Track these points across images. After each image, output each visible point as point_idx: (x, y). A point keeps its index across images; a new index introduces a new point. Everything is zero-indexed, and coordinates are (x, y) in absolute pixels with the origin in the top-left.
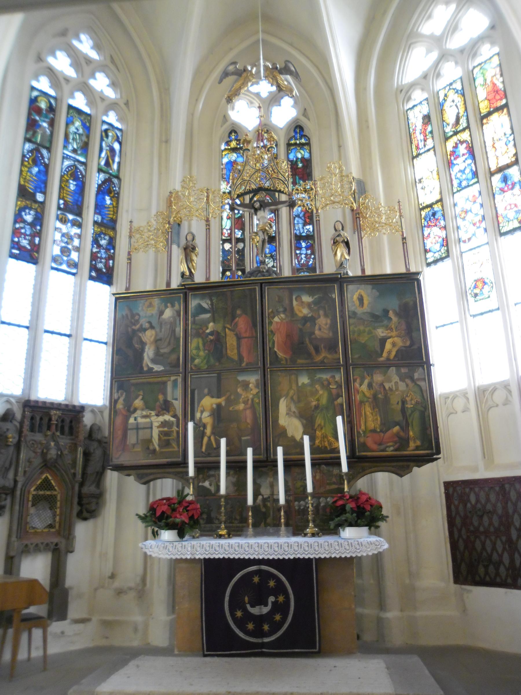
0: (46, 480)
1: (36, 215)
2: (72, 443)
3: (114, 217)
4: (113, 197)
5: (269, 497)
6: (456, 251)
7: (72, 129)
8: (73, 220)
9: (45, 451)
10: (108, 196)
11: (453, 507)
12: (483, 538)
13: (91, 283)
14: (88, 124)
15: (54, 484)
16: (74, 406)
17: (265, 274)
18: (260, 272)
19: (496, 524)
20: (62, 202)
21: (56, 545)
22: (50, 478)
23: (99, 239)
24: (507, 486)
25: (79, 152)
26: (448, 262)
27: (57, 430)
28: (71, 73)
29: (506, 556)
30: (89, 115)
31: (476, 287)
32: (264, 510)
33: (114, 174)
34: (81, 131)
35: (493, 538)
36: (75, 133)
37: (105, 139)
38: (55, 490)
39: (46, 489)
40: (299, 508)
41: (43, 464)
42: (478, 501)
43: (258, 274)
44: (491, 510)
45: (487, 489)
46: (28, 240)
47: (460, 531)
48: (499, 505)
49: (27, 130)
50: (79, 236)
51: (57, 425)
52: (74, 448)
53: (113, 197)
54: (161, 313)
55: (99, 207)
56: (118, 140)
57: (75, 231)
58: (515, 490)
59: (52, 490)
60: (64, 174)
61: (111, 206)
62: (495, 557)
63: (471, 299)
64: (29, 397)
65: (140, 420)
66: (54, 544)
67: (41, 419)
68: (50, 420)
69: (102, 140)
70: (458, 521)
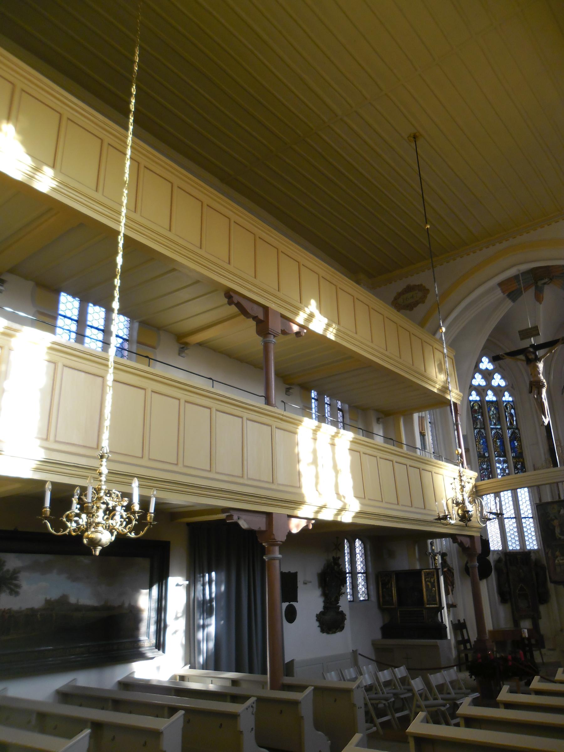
1: (487, 464)
3: (521, 451)
4: (517, 441)
7: (491, 413)
8: (503, 460)
10: (515, 441)
14: (497, 407)
16: (526, 552)
20: (496, 453)
22: (523, 586)
23: (517, 465)
25: (497, 424)
28: (483, 383)
30: (496, 401)
33: (515, 428)
34: (495, 412)
36: (493, 414)
37: (506, 410)
46: (487, 477)
49: (474, 424)
50: (508, 467)
53: (517, 441)
54: (559, 512)
55: (513, 449)
56: (512, 407)
57: (505, 465)
60: (493, 438)
61: (518, 446)
64: (506, 551)
65: (561, 561)
69: (505, 412)
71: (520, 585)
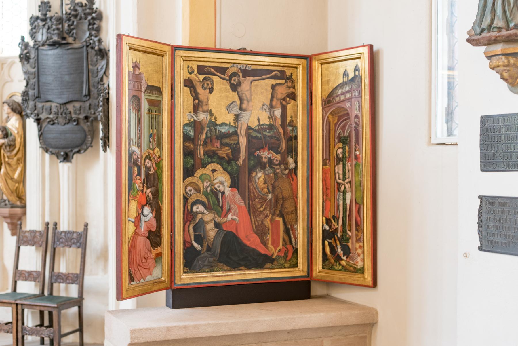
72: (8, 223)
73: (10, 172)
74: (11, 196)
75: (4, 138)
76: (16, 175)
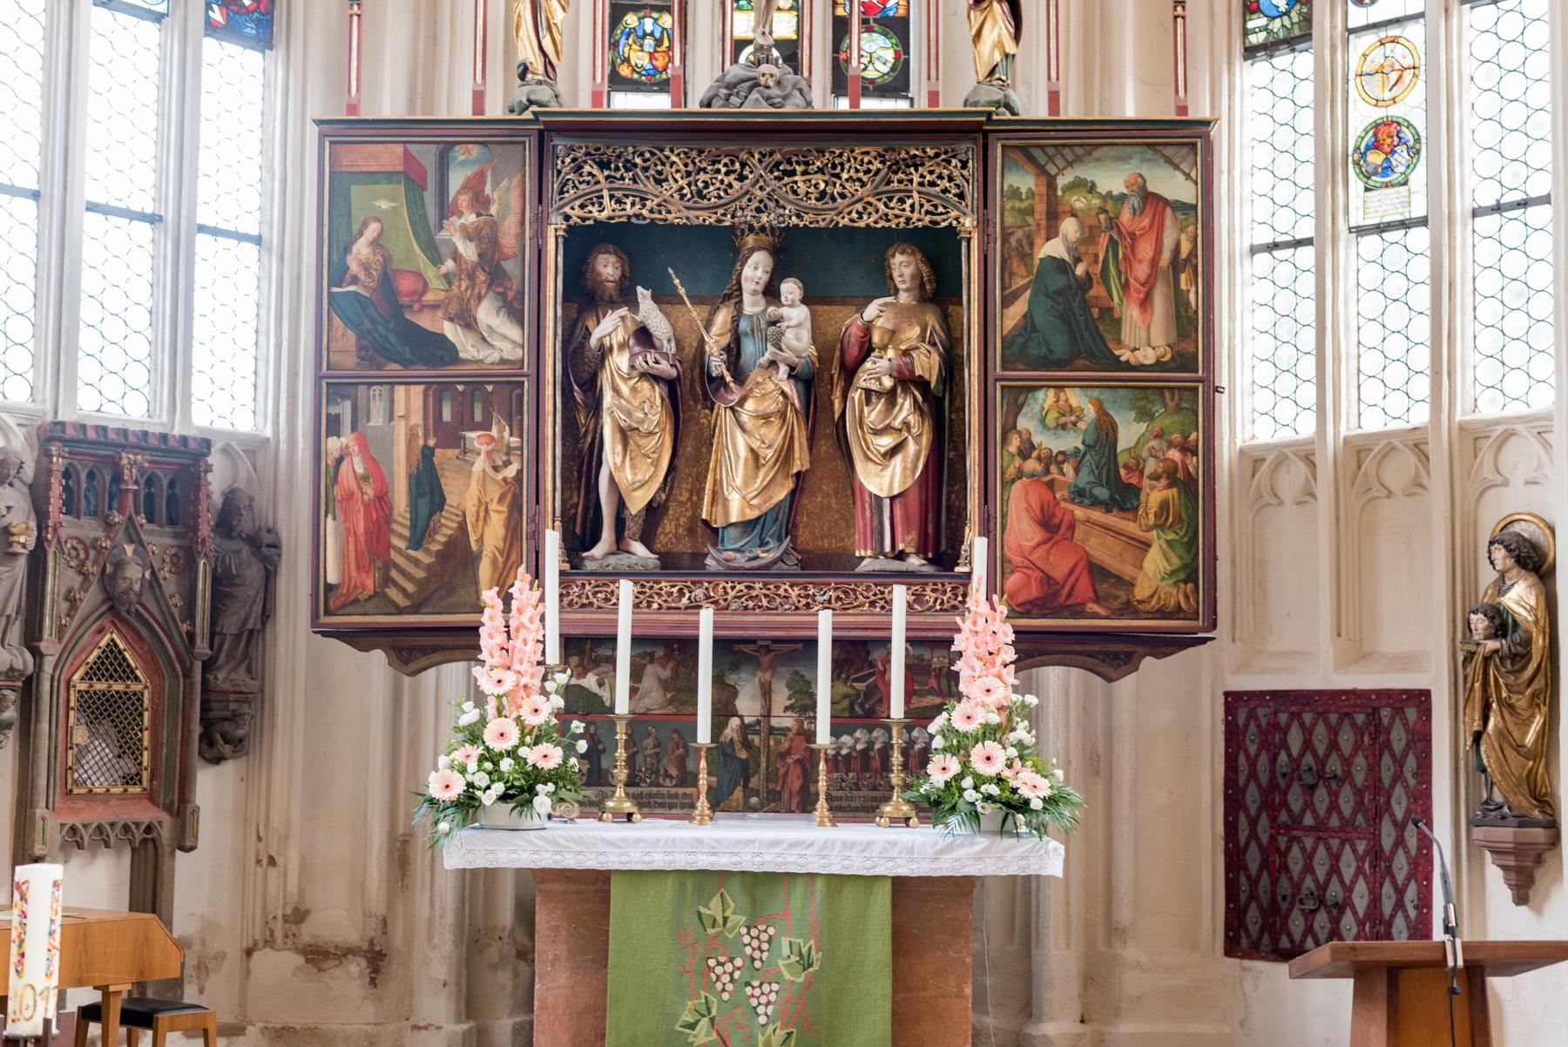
0: (111, 651)
2: (180, 547)
5: (759, 722)
6: (1333, 27)
9: (109, 569)
11: (1242, 759)
12: (1308, 842)
13: (210, 46)
15: (133, 664)
17: (775, 91)
18: (755, 84)
19: (1347, 809)
21: (149, 829)
24: (1385, 713)
26: (1303, 62)
27: (137, 513)
29: (1361, 889)
31: (1376, 145)
32: (743, 755)
35: (1335, 843)
38: (137, 678)
39: (111, 677)
40: (838, 754)
41: (104, 608)
42: (1308, 745)
43: (751, 89)
44: (1339, 772)
45: (1333, 718)
47: (1253, 823)
48: (1360, 760)
51: (136, 493)
52: (186, 562)
58: (1406, 724)
59: (128, 678)
62: (1334, 890)
63: (1356, 184)
66: (143, 827)
67: (91, 476)
68: (117, 478)
70: (1252, 796)
71: (103, 643)
72: (1504, 868)
73: (1512, 728)
74: (1515, 795)
75: (1495, 636)
76: (1530, 738)
